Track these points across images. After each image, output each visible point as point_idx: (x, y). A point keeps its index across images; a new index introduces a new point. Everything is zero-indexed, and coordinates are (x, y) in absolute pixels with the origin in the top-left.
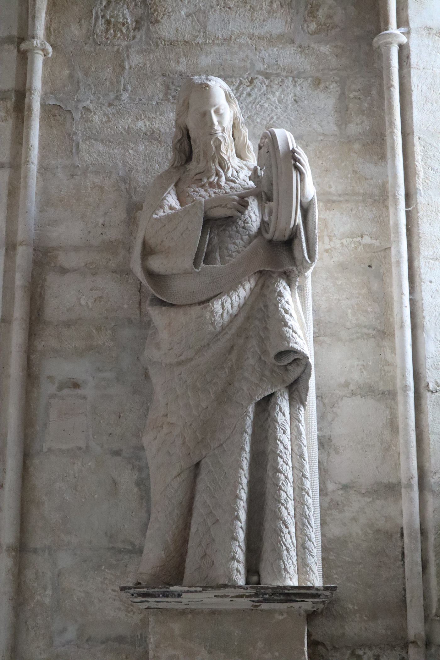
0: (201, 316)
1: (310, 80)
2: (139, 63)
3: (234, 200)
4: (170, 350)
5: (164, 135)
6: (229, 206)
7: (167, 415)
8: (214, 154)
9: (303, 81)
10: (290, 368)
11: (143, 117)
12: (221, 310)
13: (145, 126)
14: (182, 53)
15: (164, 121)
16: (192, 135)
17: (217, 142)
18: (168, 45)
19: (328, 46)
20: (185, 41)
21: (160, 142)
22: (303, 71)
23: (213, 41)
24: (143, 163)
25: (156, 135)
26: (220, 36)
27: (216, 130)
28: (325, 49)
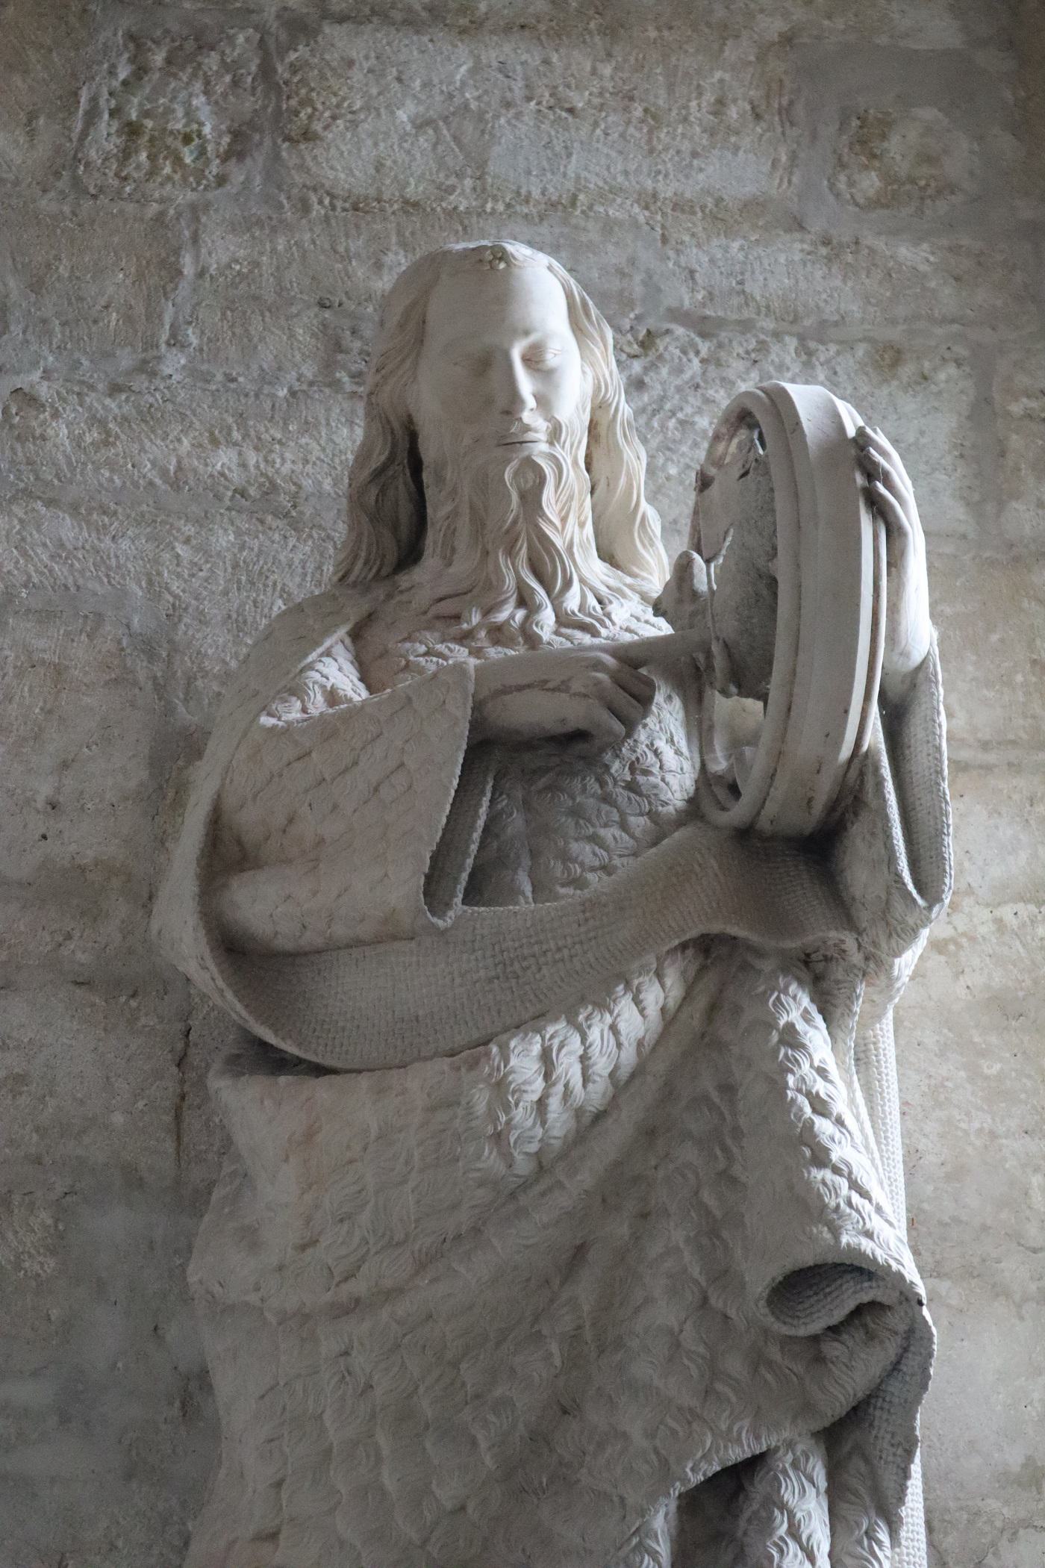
0: (451, 1103)
1: (861, 350)
2: (237, 261)
3: (598, 665)
4: (303, 1248)
5: (313, 500)
6: (576, 686)
7: (273, 1536)
8: (515, 522)
9: (838, 353)
10: (833, 1349)
11: (236, 435)
12: (539, 1084)
13: (243, 465)
14: (394, 239)
15: (317, 452)
16: (429, 453)
17: (530, 476)
18: (344, 210)
19: (925, 246)
20: (406, 202)
21: (295, 525)
22: (836, 318)
23: (508, 206)
24: (225, 593)
25: (284, 500)
26: (536, 193)
27: (527, 429)
28: (913, 255)
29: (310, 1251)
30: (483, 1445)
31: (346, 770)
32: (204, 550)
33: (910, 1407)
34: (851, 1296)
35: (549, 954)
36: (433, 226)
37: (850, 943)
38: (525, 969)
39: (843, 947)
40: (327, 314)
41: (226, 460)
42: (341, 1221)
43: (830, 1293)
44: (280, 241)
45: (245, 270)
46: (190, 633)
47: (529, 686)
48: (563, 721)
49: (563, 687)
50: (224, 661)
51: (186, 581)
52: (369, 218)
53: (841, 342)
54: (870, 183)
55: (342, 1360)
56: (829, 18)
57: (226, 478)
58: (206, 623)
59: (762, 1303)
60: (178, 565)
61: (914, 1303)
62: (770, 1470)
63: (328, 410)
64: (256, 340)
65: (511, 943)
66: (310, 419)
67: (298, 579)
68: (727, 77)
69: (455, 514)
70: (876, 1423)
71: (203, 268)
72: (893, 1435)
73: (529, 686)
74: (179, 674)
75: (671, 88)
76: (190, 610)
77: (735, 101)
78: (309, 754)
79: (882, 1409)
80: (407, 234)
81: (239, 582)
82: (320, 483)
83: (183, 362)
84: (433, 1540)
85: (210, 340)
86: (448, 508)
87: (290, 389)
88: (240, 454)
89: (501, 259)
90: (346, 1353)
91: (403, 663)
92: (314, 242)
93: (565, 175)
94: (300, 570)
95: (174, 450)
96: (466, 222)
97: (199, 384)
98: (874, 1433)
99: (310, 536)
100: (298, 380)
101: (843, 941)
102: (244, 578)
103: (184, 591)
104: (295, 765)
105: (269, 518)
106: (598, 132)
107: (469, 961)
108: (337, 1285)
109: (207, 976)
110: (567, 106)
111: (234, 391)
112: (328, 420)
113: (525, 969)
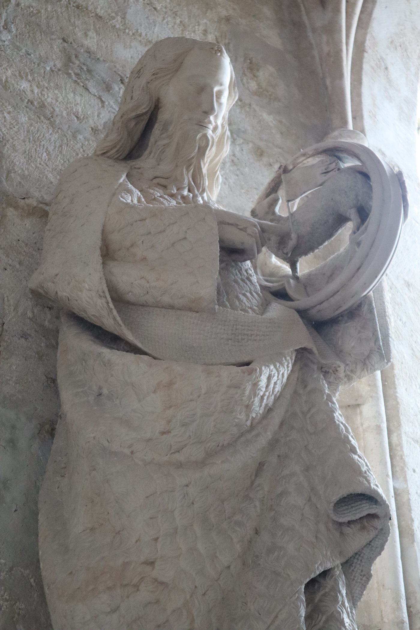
0: (237, 387)
1: (251, 145)
2: (32, 7)
3: (255, 226)
4: (163, 433)
5: (59, 118)
6: (249, 231)
7: (152, 564)
8: (193, 158)
9: (243, 143)
10: (347, 530)
11: (30, 78)
12: (264, 390)
13: (32, 91)
14: (92, 27)
15: (60, 99)
16: (163, 116)
17: (204, 141)
18: (73, 6)
19: (272, 116)
20: (97, 15)
21: (52, 124)
22: (243, 129)
23: (133, 34)
24: (24, 141)
25: (48, 113)
26: (144, 34)
27: (210, 122)
28: (268, 118)
29: (165, 436)
30: (235, 540)
31: (160, 232)
32: (15, 119)
33: (371, 560)
34: (366, 509)
35: (253, 336)
36: (107, 29)
37: (342, 369)
38: (243, 339)
39: (338, 369)
40: (66, 45)
41: (25, 86)
42: (183, 425)
43: (354, 507)
44: (49, 7)
45: (35, 12)
46: (9, 152)
47: (232, 224)
48: (243, 243)
49: (244, 230)
50: (22, 169)
51: (8, 130)
52: (83, 14)
53: (244, 139)
54: (253, 85)
55: (185, 488)
56: (241, 18)
57: (25, 93)
58: (16, 151)
59: (332, 504)
60: (5, 121)
61: (388, 518)
62: (332, 576)
63: (66, 83)
64: (38, 42)
65: (240, 327)
66: (58, 84)
67: (53, 148)
68: (208, 22)
69: (166, 145)
70: (354, 565)
71: (18, 3)
72: (362, 571)
73: (232, 224)
74: (4, 167)
75: (189, 17)
76: (10, 142)
77: (211, 33)
78: (145, 220)
79: (358, 559)
80: (97, 27)
81: (30, 139)
82: (62, 112)
83: (9, 38)
84: (221, 579)
85: (20, 34)
86: (165, 142)
87: (51, 68)
88: (31, 86)
89: (220, 51)
90: (187, 486)
91: (153, 197)
92: (62, 13)
93: (153, 32)
94: (53, 144)
95: (5, 72)
96: (119, 33)
97: (16, 50)
98: (352, 568)
99: (58, 132)
100: (54, 66)
101: (339, 367)
102: (31, 138)
103: (7, 134)
104: (139, 222)
105: (42, 118)
106: (165, 21)
107: (221, 329)
108: (171, 454)
109: (104, 300)
110: (154, 6)
111: (30, 59)
112: (65, 87)
113: (243, 339)
